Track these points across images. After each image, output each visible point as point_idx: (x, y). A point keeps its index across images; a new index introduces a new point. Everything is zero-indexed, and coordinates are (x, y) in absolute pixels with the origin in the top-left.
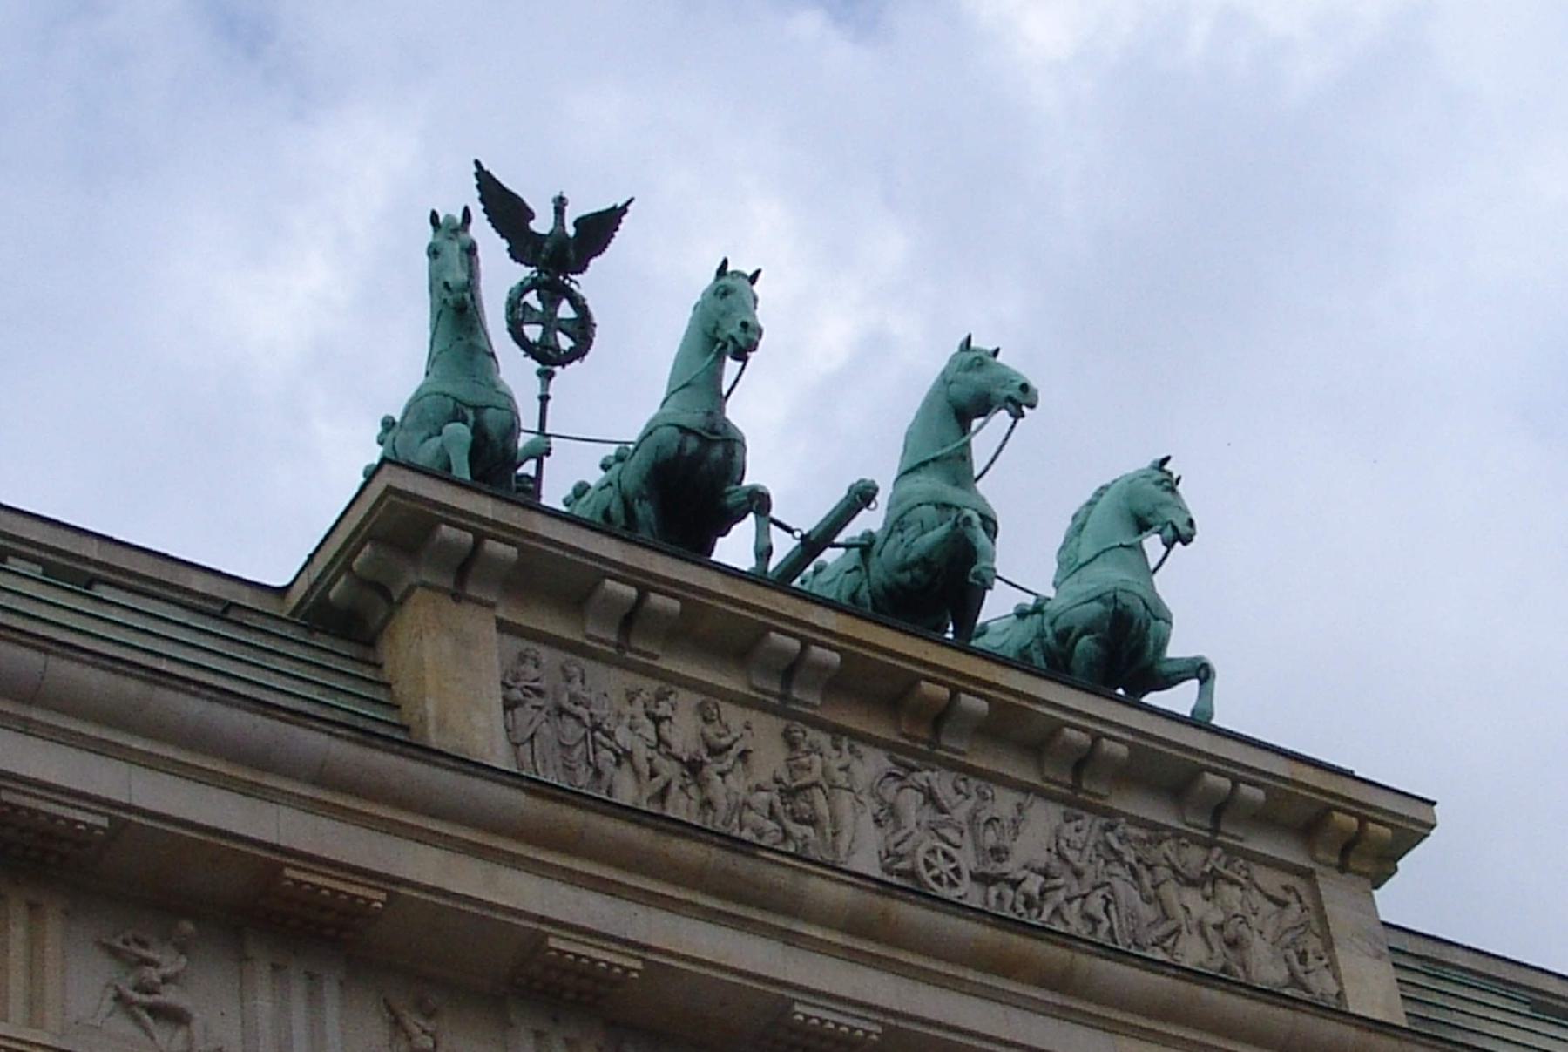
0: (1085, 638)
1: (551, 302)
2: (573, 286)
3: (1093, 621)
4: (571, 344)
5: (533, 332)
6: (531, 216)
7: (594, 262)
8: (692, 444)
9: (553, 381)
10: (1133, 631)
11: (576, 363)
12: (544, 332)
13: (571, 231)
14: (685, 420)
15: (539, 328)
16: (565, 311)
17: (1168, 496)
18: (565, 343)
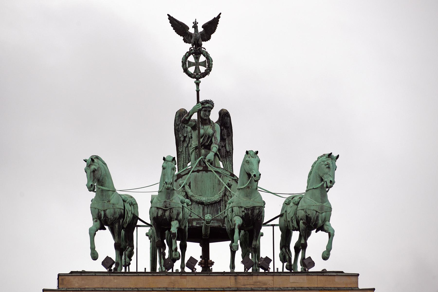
0: (301, 222)
1: (197, 58)
2: (203, 49)
3: (302, 217)
4: (206, 69)
5: (192, 70)
6: (189, 29)
7: (212, 36)
8: (160, 212)
9: (200, 84)
10: (312, 220)
11: (207, 76)
12: (196, 68)
13: (200, 29)
14: (158, 206)
15: (194, 67)
16: (202, 59)
17: (327, 170)
18: (203, 69)
